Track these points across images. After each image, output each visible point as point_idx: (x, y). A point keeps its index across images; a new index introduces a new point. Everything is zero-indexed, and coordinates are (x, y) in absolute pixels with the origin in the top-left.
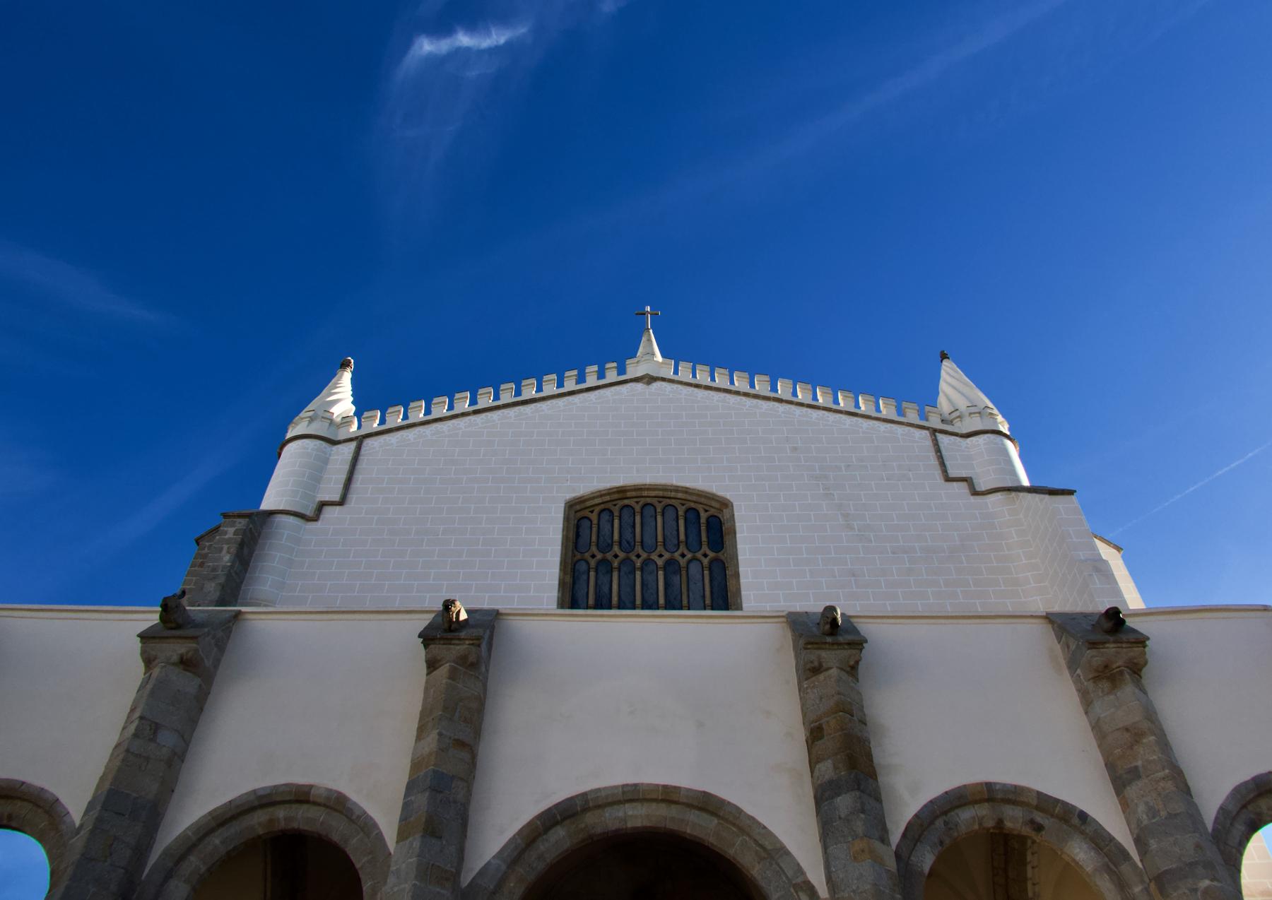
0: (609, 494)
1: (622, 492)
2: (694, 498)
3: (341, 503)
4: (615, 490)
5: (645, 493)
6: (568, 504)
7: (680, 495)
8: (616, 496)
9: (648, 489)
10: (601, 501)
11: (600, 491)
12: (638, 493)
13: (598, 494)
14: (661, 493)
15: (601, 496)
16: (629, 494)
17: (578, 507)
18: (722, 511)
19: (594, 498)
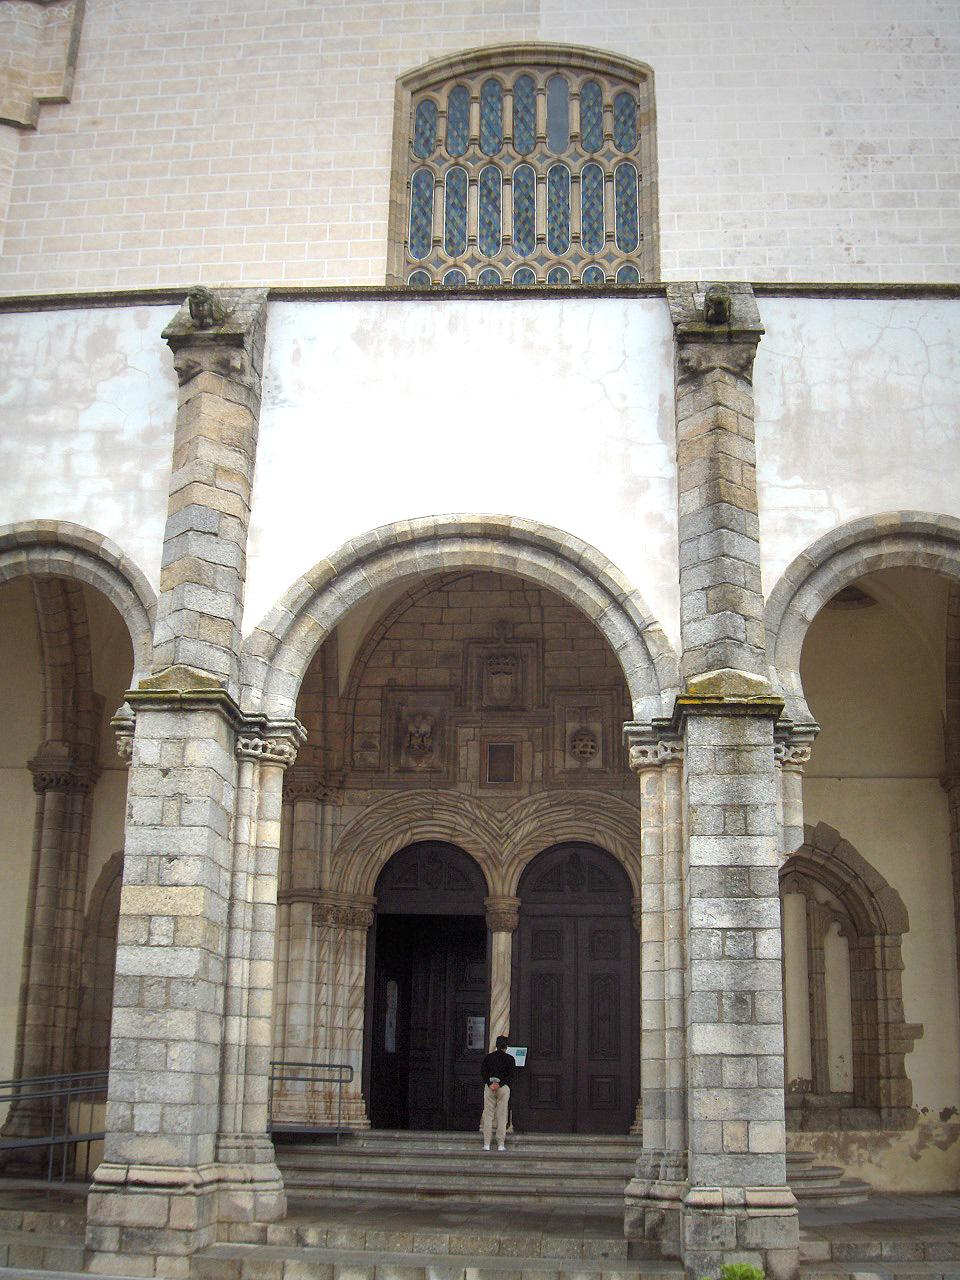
0: (463, 62)
1: (481, 62)
2: (596, 66)
3: (64, 101)
4: (473, 55)
5: (518, 59)
6: (400, 82)
7: (574, 62)
8: (473, 66)
9: (523, 53)
10: (451, 74)
11: (449, 58)
12: (510, 60)
13: (447, 62)
14: (543, 59)
15: (451, 65)
16: (494, 62)
17: (416, 85)
18: (638, 85)
19: (439, 69)
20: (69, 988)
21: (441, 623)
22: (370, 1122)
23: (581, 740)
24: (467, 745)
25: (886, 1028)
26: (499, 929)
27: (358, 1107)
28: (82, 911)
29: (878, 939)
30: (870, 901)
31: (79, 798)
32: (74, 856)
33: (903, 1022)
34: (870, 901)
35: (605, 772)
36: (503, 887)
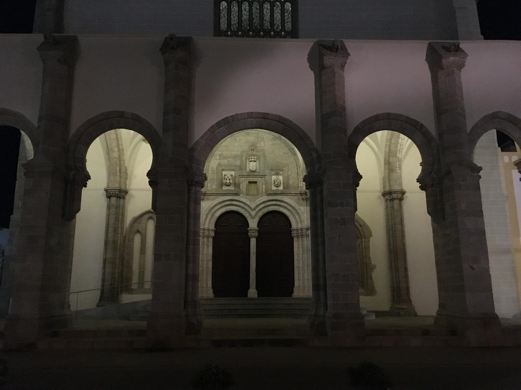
20: (119, 258)
21: (234, 146)
22: (214, 295)
23: (277, 181)
24: (242, 183)
25: (366, 265)
26: (252, 238)
27: (211, 291)
28: (123, 234)
29: (363, 239)
30: (361, 228)
31: (122, 200)
32: (120, 217)
33: (371, 263)
34: (361, 228)
35: (284, 190)
36: (253, 224)
